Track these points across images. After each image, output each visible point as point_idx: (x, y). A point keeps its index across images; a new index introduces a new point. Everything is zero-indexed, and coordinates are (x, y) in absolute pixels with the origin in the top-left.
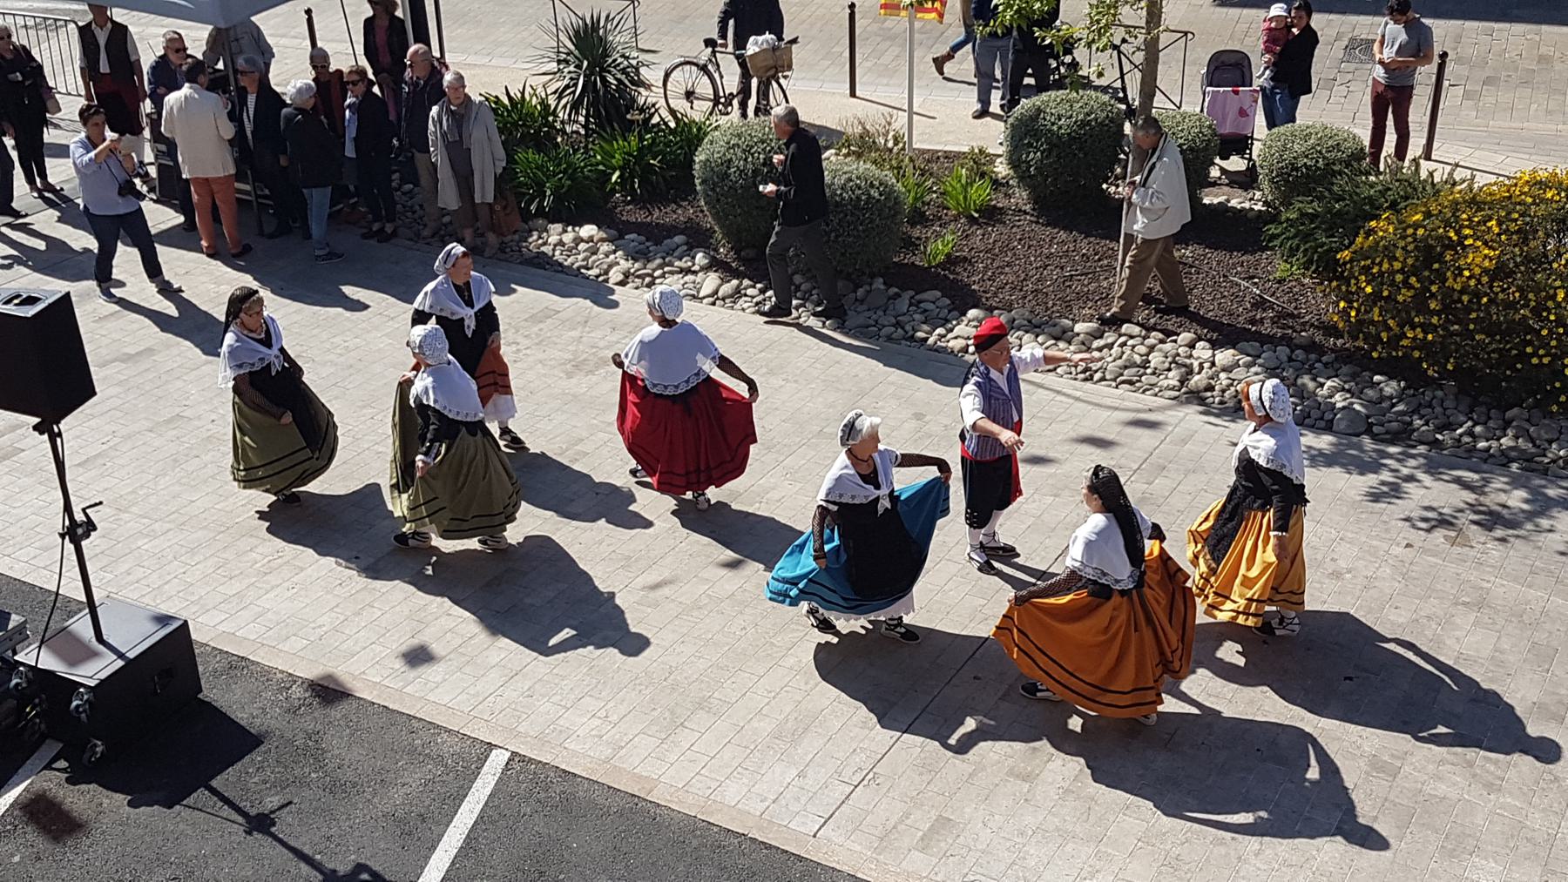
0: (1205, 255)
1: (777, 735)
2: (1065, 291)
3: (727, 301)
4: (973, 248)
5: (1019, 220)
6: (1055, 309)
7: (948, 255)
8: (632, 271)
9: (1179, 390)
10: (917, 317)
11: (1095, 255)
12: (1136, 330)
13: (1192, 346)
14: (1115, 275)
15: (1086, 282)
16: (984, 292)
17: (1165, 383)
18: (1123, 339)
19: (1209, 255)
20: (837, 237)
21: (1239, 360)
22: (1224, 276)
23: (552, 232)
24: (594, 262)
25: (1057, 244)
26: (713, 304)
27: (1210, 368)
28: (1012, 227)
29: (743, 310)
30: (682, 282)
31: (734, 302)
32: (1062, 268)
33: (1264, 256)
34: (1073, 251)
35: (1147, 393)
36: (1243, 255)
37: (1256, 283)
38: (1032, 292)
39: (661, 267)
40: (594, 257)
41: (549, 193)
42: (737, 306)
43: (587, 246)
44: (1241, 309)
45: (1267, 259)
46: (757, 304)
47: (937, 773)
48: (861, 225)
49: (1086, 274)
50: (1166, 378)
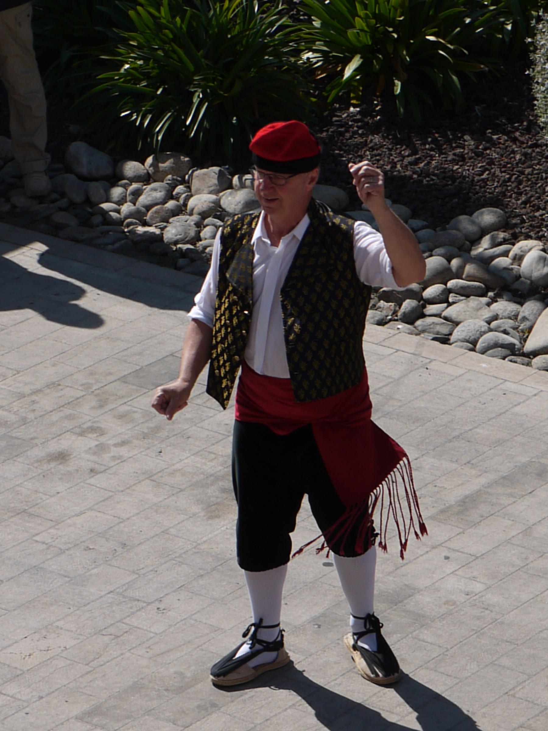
23: (195, 184)
30: (487, 313)
41: (196, 100)
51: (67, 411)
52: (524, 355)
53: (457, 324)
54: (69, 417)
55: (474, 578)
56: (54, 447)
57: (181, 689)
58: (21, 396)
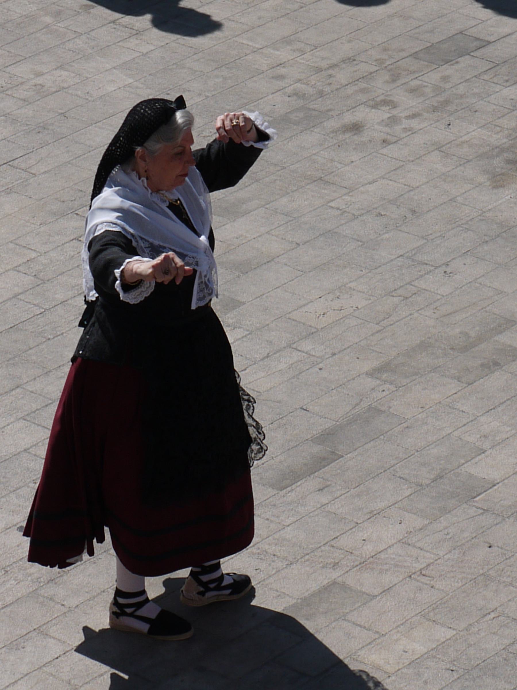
51: (362, 85)
54: (363, 91)
56: (349, 118)
57: (464, 349)
58: (319, 70)
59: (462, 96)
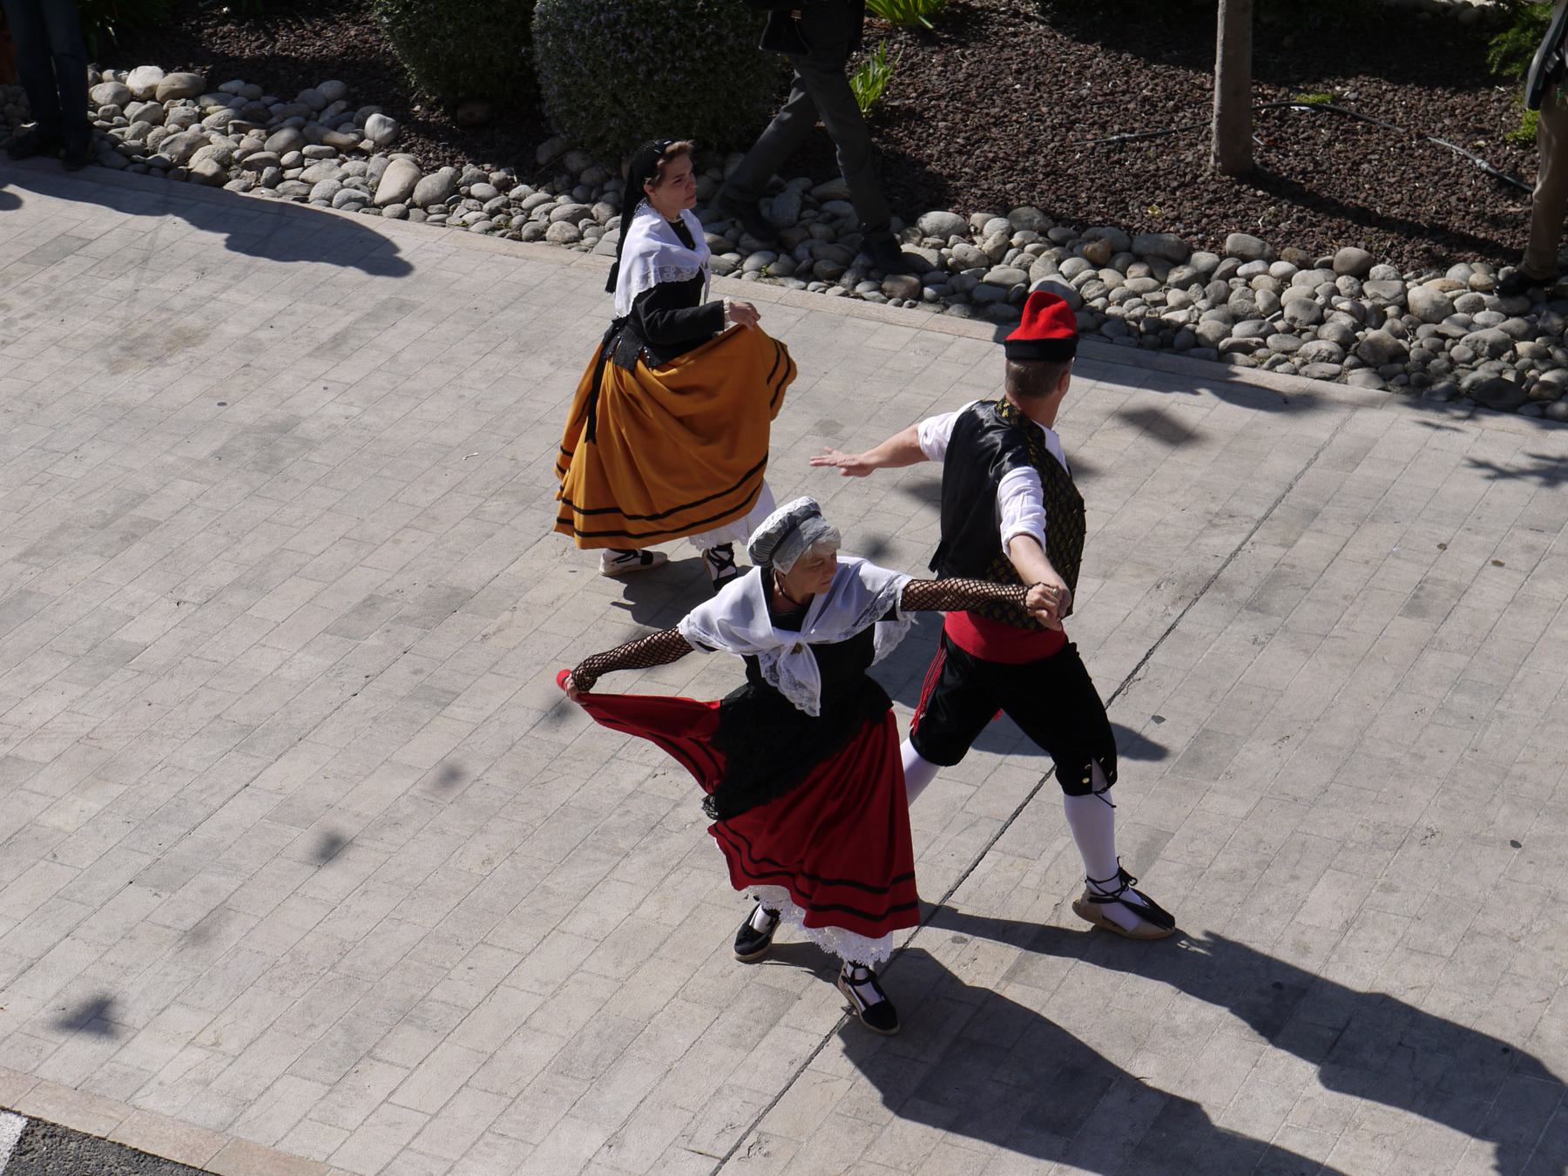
0: (1381, 96)
1: (563, 1067)
2: (1109, 171)
3: (433, 208)
4: (926, 91)
5: (1015, 35)
6: (1092, 207)
7: (877, 106)
8: (236, 154)
9: (1340, 362)
10: (819, 229)
11: (1168, 99)
12: (1253, 243)
13: (1361, 273)
14: (1208, 138)
15: (1151, 153)
16: (951, 177)
17: (1312, 347)
18: (1228, 264)
19: (1389, 96)
20: (650, 73)
21: (1453, 299)
22: (1420, 136)
24: (159, 138)
25: (1092, 79)
26: (404, 216)
27: (1399, 316)
28: (1002, 48)
29: (465, 225)
30: (339, 173)
31: (446, 212)
32: (1103, 127)
33: (1494, 96)
34: (1124, 93)
35: (1279, 368)
36: (1453, 94)
37: (1480, 149)
38: (1047, 175)
39: (296, 144)
40: (158, 130)
42: (454, 219)
43: (144, 107)
44: (1453, 199)
45: (1499, 100)
46: (493, 213)
47: (885, 1127)
48: (699, 46)
49: (1152, 137)
50: (1315, 337)
52: (375, 206)
53: (313, 184)
55: (351, 404)
57: (104, 526)
59: (71, 293)
